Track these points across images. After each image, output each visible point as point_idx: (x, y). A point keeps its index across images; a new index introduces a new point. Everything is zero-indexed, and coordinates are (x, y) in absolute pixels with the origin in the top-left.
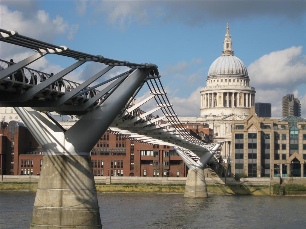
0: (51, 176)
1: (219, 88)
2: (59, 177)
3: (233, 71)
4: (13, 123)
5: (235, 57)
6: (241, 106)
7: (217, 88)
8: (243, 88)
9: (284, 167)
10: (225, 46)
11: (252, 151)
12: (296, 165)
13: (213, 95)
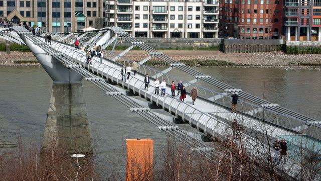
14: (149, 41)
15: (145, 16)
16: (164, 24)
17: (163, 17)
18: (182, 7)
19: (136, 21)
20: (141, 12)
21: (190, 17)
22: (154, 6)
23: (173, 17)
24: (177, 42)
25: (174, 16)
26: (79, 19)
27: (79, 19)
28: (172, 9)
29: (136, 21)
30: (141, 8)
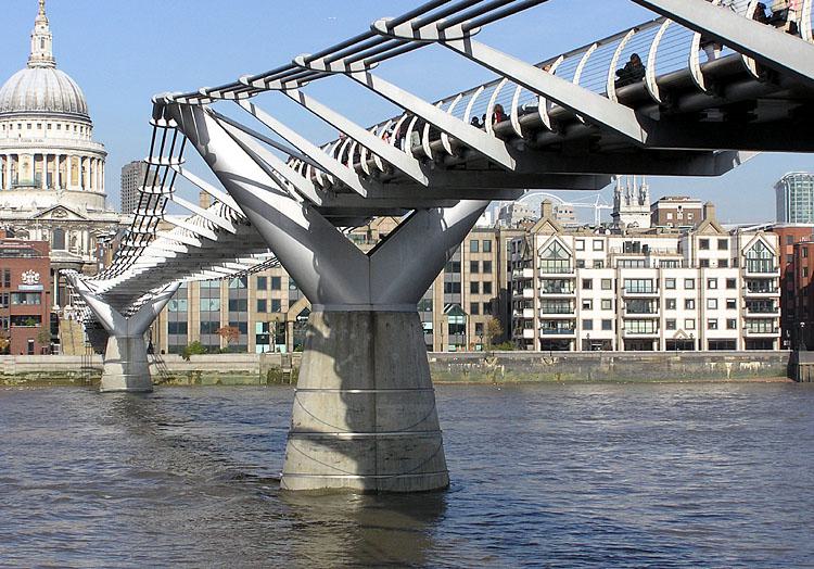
0: (343, 360)
1: (26, 144)
2: (365, 365)
3: (60, 104)
5: (59, 72)
6: (75, 188)
7: (19, 143)
8: (79, 145)
9: (282, 326)
10: (36, 43)
13: (9, 158)
18: (693, 280)
19: (585, 315)
20: (597, 294)
22: (625, 279)
23: (671, 304)
24: (684, 360)
25: (674, 300)
26: (452, 320)
27: (452, 320)
28: (671, 284)
29: (585, 315)
30: (596, 284)
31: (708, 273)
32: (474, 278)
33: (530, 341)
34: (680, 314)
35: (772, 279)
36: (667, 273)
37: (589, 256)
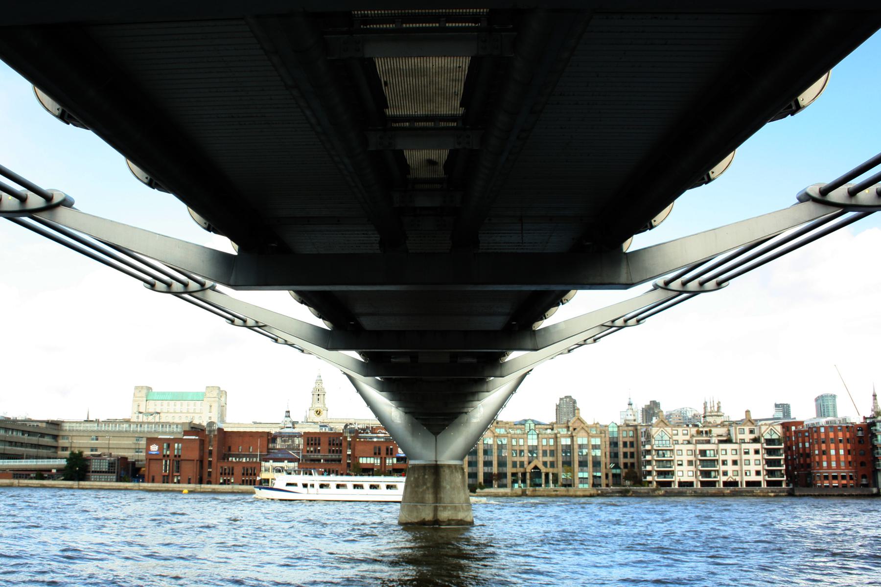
2: (431, 491)
4: (211, 424)
9: (524, 474)
11: (488, 458)
12: (536, 473)
14: (695, 492)
15: (690, 463)
16: (715, 471)
17: (713, 462)
21: (747, 462)
23: (724, 463)
26: (614, 471)
28: (724, 452)
30: (684, 452)
31: (744, 446)
32: (625, 450)
33: (650, 482)
34: (730, 468)
35: (779, 449)
36: (722, 446)
37: (681, 438)
